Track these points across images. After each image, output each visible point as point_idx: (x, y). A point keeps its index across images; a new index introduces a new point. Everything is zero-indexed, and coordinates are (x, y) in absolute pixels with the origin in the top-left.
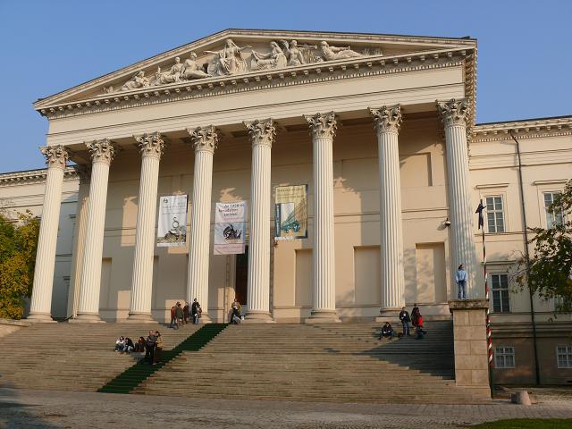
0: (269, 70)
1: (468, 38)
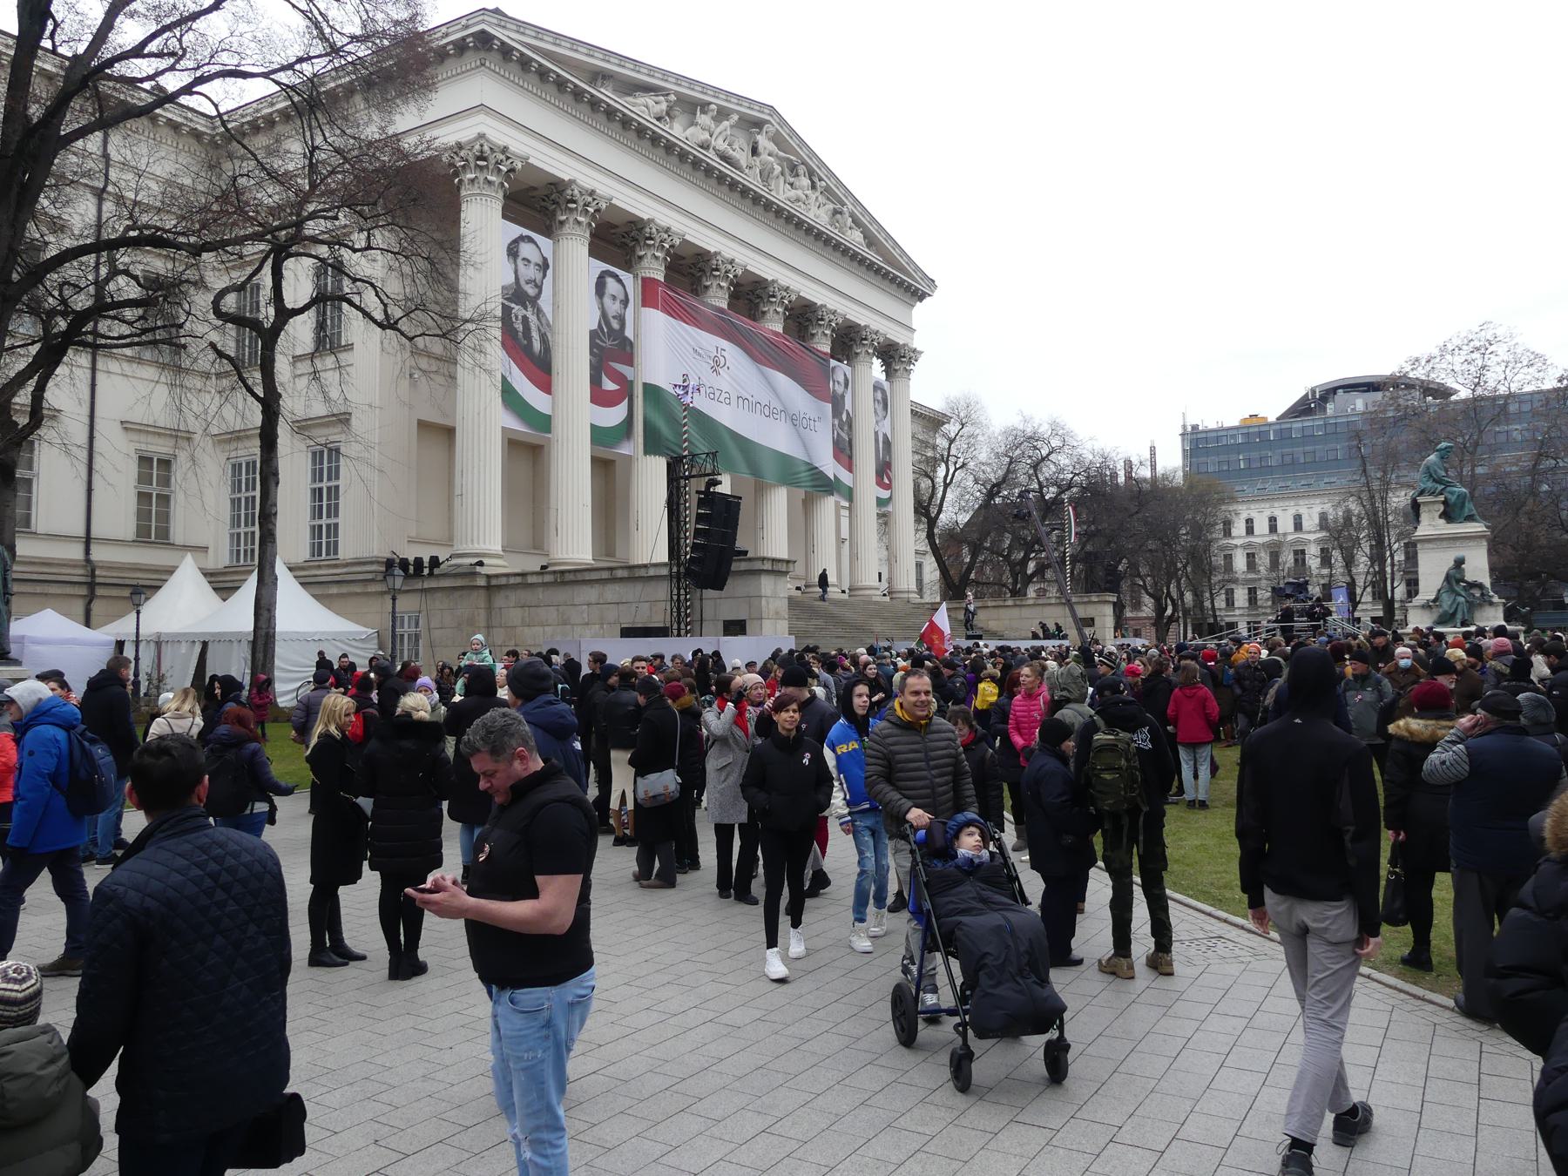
0: (799, 210)
1: (933, 281)
